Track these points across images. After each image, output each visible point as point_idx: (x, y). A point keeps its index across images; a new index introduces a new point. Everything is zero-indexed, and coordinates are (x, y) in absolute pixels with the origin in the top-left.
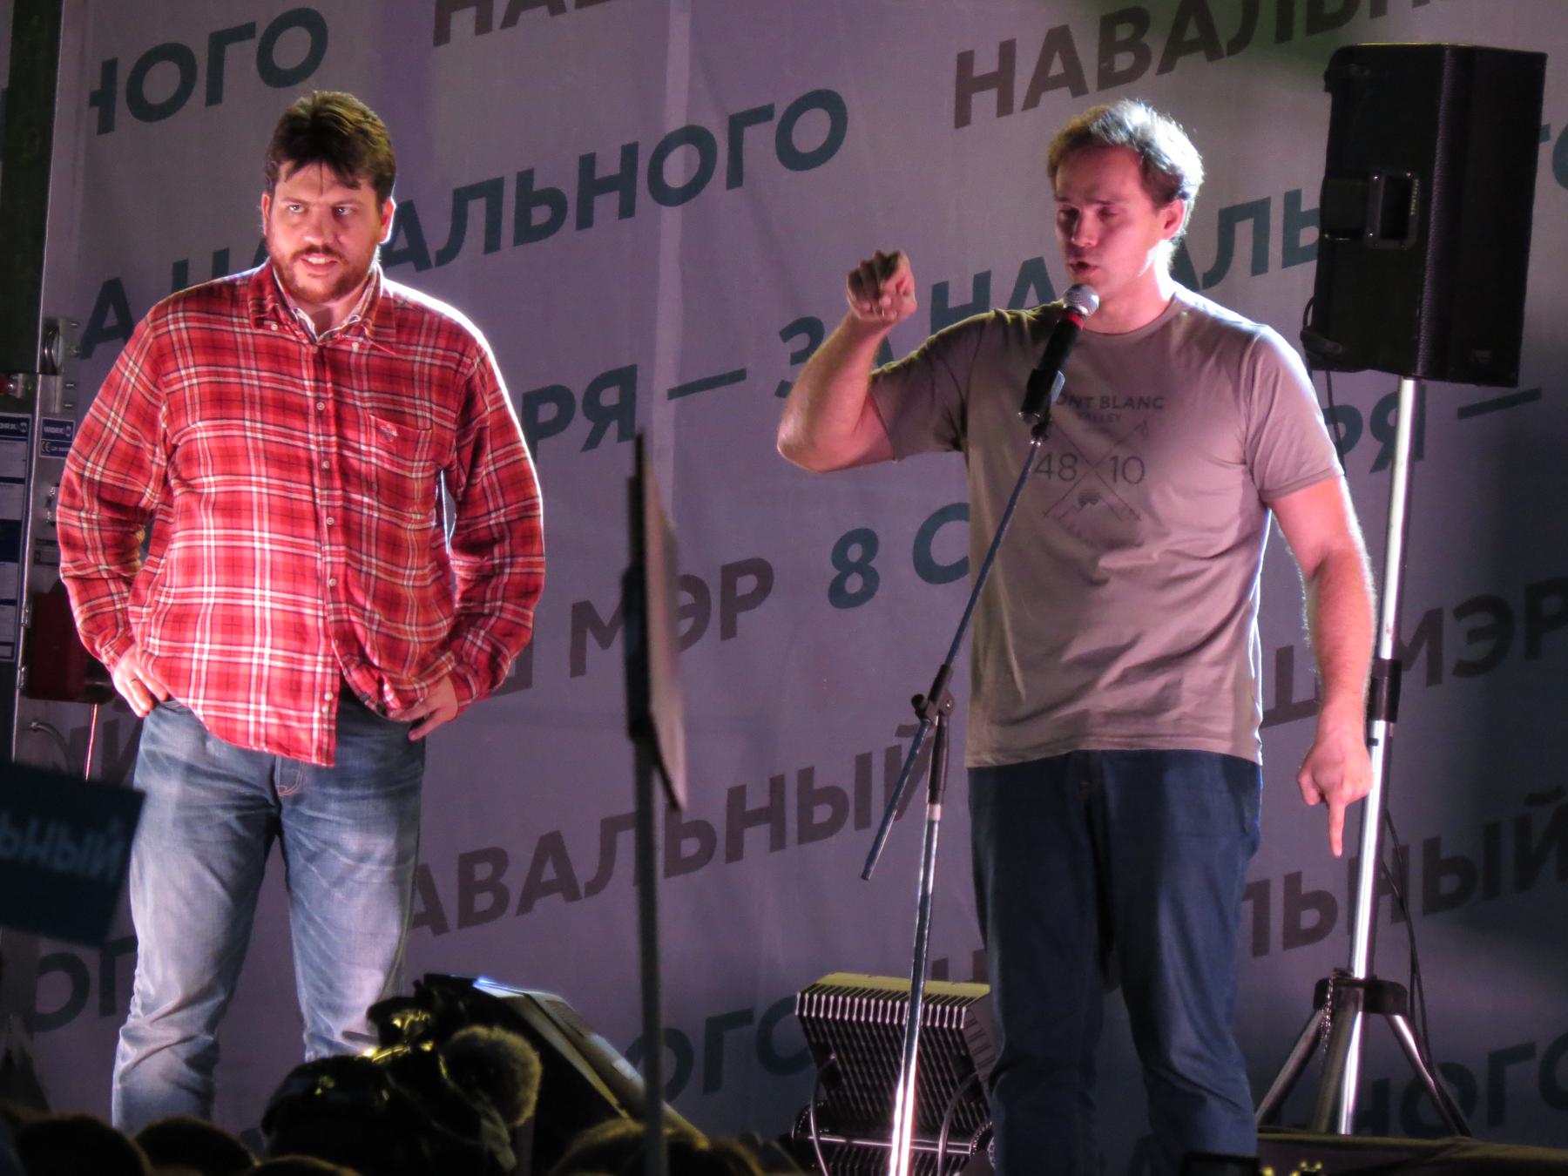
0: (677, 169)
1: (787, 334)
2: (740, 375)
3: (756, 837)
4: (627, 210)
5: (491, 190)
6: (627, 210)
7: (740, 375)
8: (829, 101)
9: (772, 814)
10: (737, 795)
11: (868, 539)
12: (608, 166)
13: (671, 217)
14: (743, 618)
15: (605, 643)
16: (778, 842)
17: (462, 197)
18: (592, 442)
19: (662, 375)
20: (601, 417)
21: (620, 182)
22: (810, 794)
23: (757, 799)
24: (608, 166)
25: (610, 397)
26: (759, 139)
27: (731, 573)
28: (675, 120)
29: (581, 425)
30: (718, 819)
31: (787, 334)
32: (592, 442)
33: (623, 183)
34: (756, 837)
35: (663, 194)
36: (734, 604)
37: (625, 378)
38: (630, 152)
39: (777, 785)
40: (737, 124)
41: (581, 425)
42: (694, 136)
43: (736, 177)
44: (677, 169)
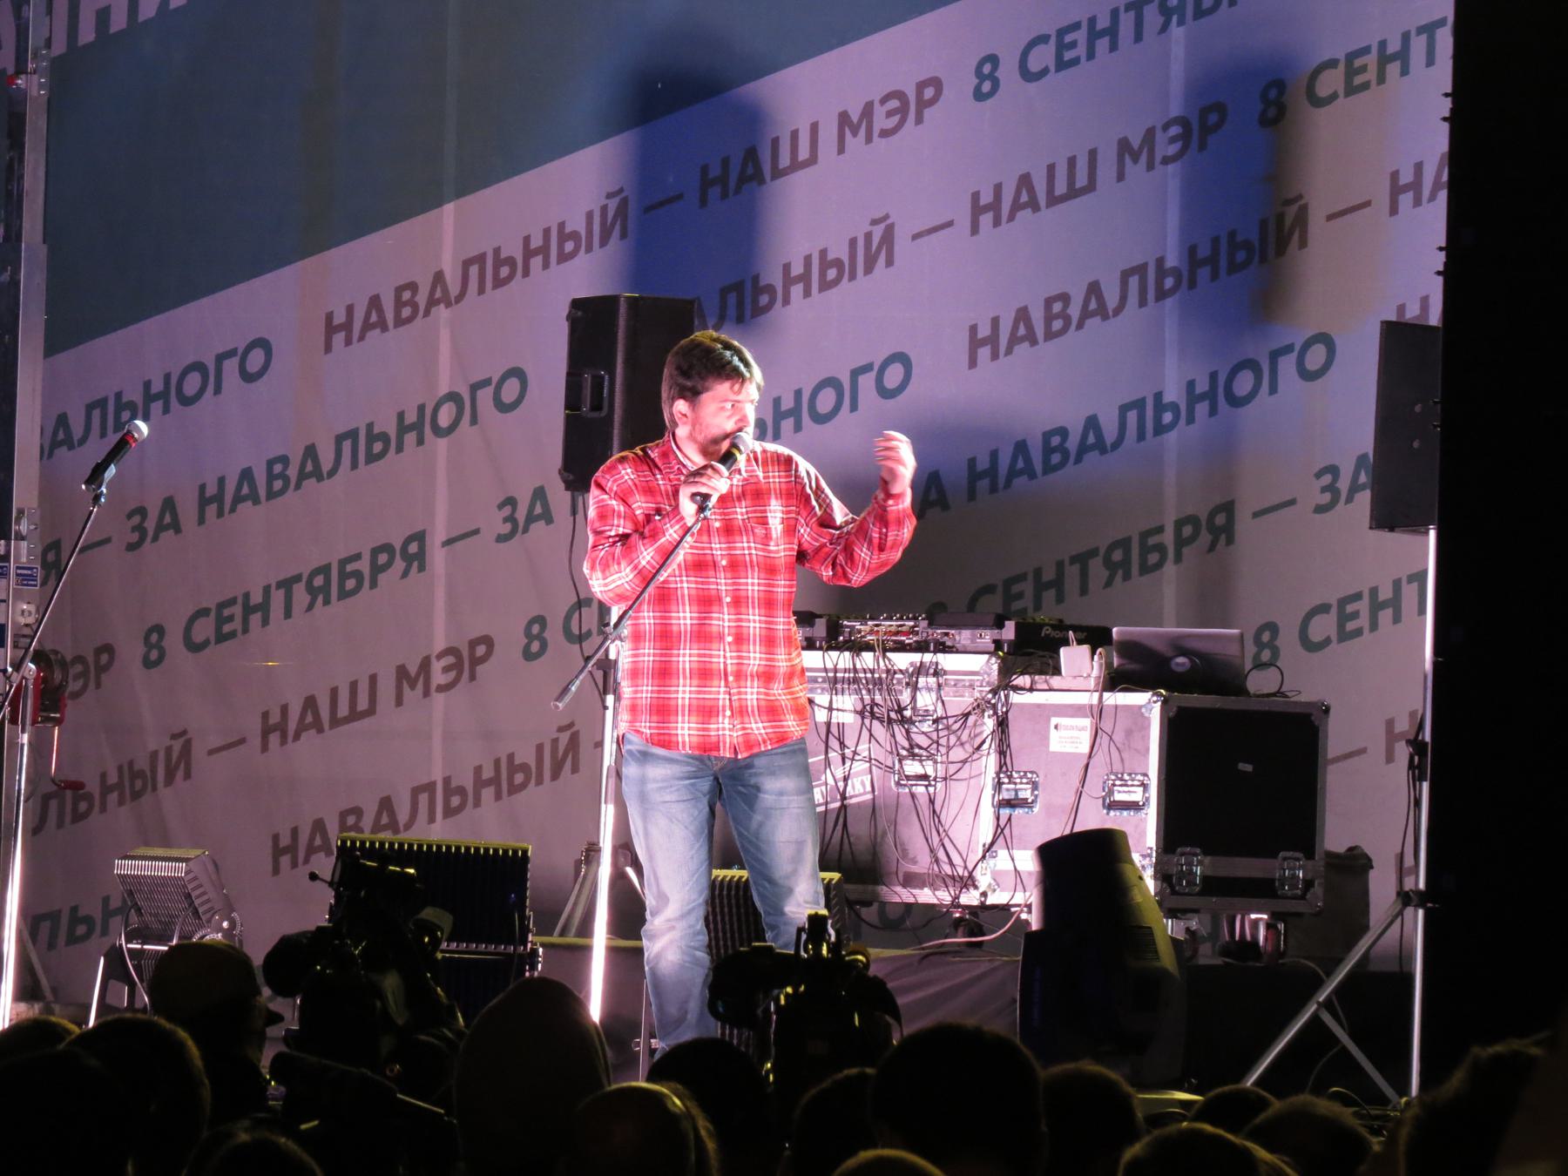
0: (444, 419)
1: (501, 506)
2: (476, 532)
3: (488, 793)
4: (420, 442)
5: (353, 434)
6: (420, 442)
7: (476, 532)
8: (518, 373)
9: (495, 781)
10: (478, 770)
11: (541, 620)
12: (411, 417)
13: (442, 443)
14: (479, 669)
15: (413, 687)
16: (498, 797)
17: (339, 440)
18: (405, 574)
19: (439, 534)
20: (409, 559)
21: (417, 426)
22: (513, 768)
23: (488, 773)
24: (411, 417)
25: (413, 548)
26: (485, 395)
27: (473, 644)
28: (443, 390)
29: (399, 564)
30: (469, 785)
31: (501, 506)
32: (405, 574)
33: (418, 426)
34: (488, 793)
35: (438, 431)
36: (476, 662)
37: (420, 537)
38: (421, 408)
39: (497, 762)
40: (475, 388)
41: (399, 564)
42: (453, 397)
43: (474, 420)
44: (444, 419)
